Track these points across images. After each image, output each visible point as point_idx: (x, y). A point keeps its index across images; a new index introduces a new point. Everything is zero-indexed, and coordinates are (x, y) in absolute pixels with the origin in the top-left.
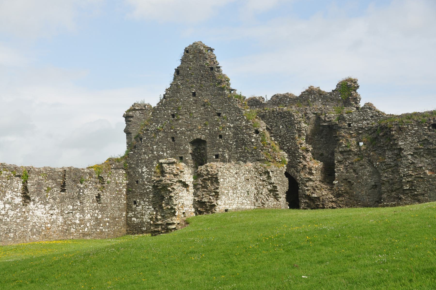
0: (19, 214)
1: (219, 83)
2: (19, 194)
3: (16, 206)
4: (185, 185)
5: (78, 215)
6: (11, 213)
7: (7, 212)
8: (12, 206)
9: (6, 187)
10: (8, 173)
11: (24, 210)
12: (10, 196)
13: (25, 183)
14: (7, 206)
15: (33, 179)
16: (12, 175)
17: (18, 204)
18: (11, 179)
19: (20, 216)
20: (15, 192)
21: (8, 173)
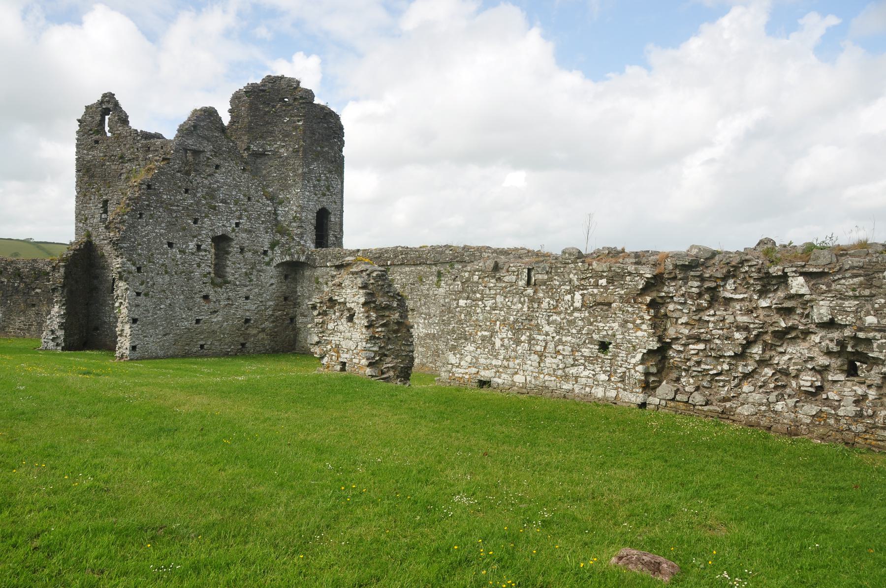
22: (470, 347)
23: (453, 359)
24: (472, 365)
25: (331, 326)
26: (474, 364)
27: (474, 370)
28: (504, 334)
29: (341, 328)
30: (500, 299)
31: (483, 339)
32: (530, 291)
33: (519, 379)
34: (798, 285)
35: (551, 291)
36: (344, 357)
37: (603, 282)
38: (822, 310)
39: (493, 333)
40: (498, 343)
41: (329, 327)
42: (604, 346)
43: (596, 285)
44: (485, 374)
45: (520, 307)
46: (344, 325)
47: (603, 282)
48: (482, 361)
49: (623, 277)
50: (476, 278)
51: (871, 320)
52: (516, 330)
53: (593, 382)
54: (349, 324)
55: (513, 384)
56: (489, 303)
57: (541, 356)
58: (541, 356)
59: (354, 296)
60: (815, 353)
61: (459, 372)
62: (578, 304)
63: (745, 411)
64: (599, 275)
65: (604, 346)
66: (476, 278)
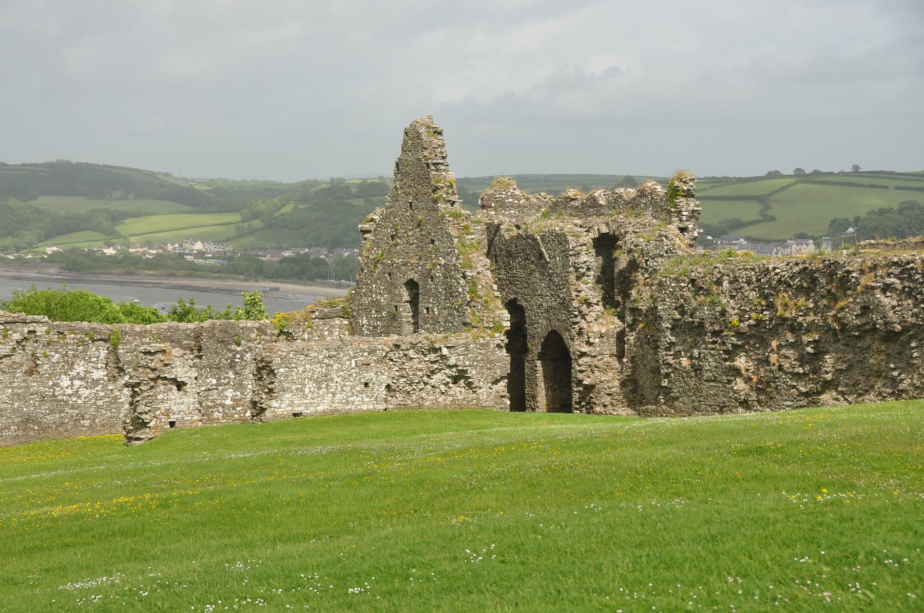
0: (102, 394)
1: (434, 191)
2: (99, 366)
3: (95, 383)
4: (180, 386)
5: (229, 393)
6: (85, 392)
7: (77, 392)
8: (87, 382)
9: (74, 356)
10: (78, 337)
11: (110, 388)
12: (82, 368)
13: (114, 351)
14: (77, 383)
15: (128, 342)
16: (87, 339)
17: (98, 380)
18: (83, 345)
19: (104, 397)
20: (93, 362)
21: (78, 337)
22: (288, 395)
23: (274, 403)
24: (289, 405)
25: (160, 397)
26: (292, 404)
27: (290, 408)
28: (310, 386)
29: (172, 397)
30: (308, 366)
31: (297, 389)
32: (326, 361)
33: (320, 408)
34: (445, 351)
35: (339, 360)
36: (173, 418)
37: (366, 354)
38: (452, 361)
39: (304, 385)
40: (307, 390)
41: (159, 397)
42: (366, 385)
43: (362, 356)
44: (298, 410)
45: (319, 370)
46: (174, 393)
47: (366, 354)
48: (296, 402)
49: (375, 351)
50: (291, 355)
51: (467, 363)
52: (318, 383)
53: (363, 403)
54: (181, 393)
55: (317, 412)
56: (301, 369)
57: (334, 394)
58: (334, 394)
59: (186, 373)
60: (444, 377)
61: (279, 412)
62: (353, 365)
63: (427, 403)
64: (363, 351)
65: (366, 385)
66: (291, 355)
